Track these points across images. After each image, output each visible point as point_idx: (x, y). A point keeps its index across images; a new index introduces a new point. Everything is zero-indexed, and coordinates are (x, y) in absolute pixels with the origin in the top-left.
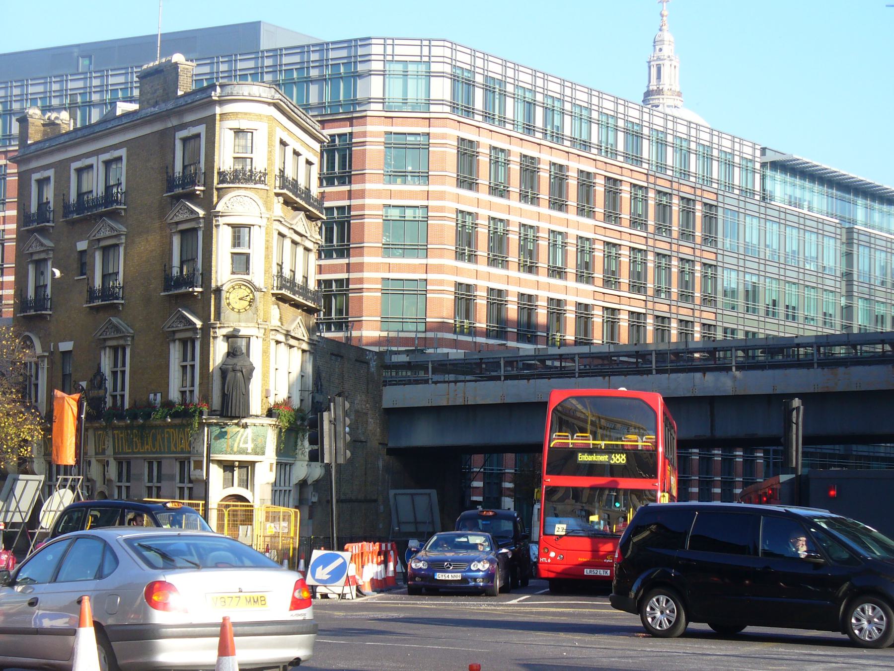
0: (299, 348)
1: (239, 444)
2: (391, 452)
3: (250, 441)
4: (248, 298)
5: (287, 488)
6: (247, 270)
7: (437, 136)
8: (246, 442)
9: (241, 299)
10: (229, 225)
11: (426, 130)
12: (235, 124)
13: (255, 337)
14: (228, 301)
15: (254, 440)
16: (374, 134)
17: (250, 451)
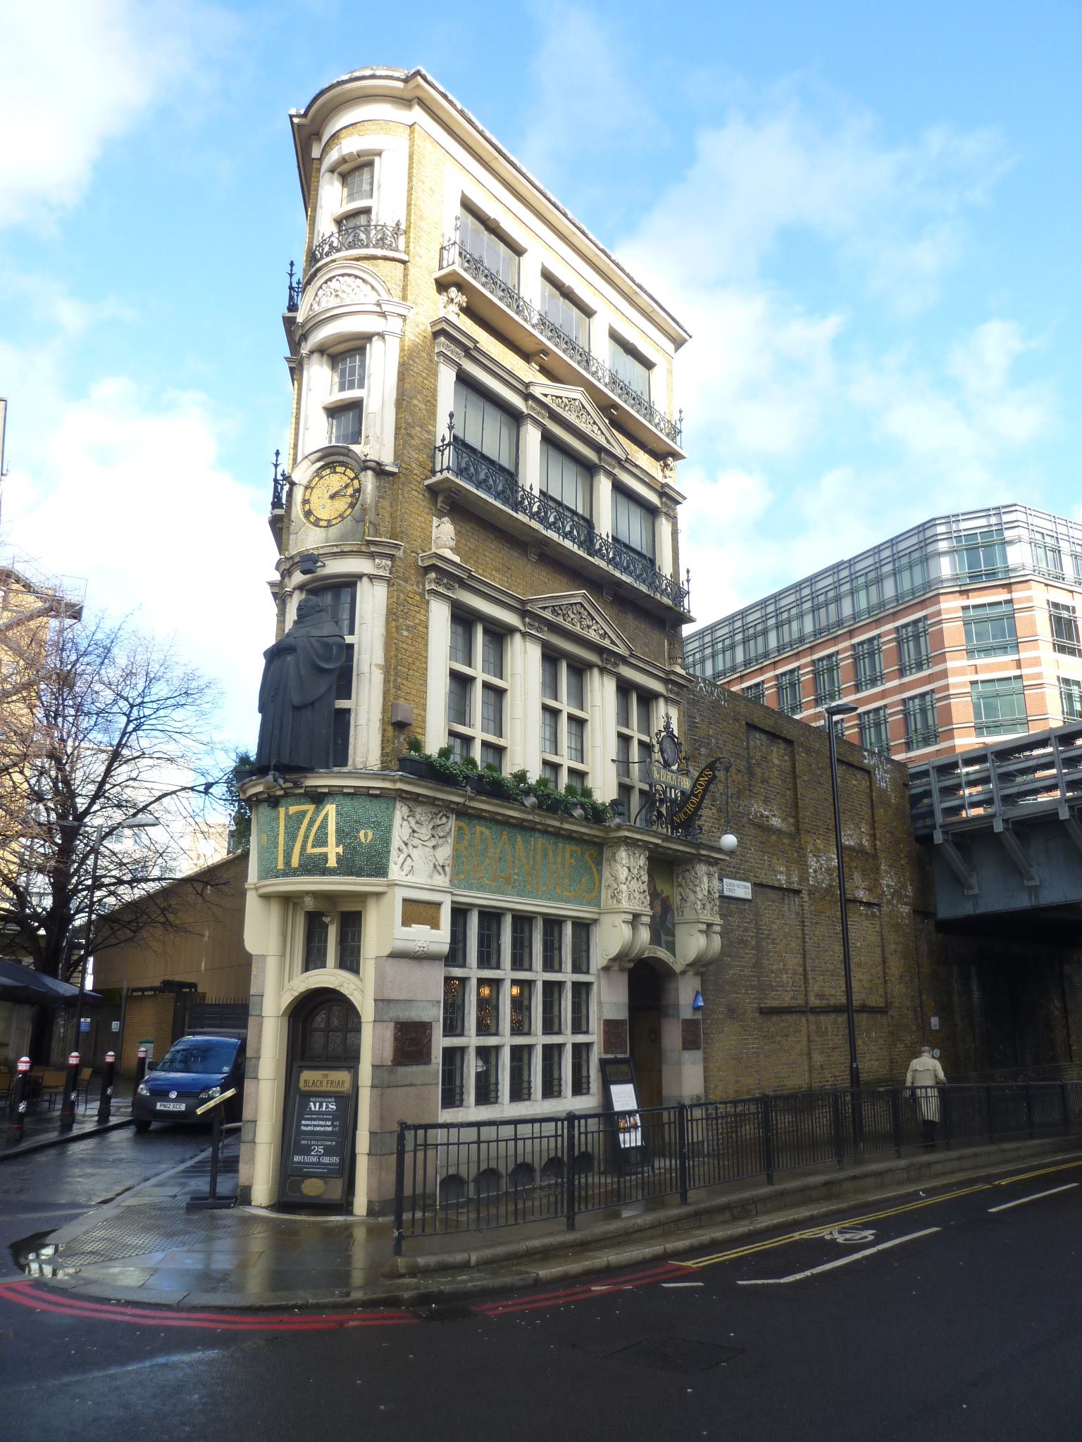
0: (603, 670)
1: (304, 847)
2: (945, 927)
3: (332, 838)
4: (350, 491)
5: (567, 976)
6: (356, 437)
7: (1020, 600)
8: (321, 841)
9: (332, 497)
10: (321, 350)
11: (1008, 597)
12: (333, 156)
13: (365, 579)
14: (307, 507)
15: (341, 835)
16: (949, 611)
17: (332, 862)
